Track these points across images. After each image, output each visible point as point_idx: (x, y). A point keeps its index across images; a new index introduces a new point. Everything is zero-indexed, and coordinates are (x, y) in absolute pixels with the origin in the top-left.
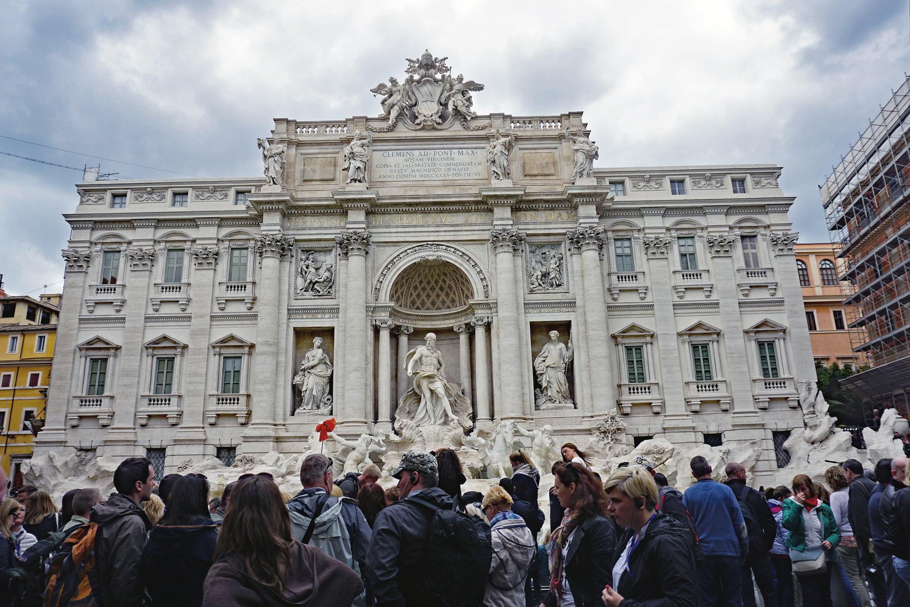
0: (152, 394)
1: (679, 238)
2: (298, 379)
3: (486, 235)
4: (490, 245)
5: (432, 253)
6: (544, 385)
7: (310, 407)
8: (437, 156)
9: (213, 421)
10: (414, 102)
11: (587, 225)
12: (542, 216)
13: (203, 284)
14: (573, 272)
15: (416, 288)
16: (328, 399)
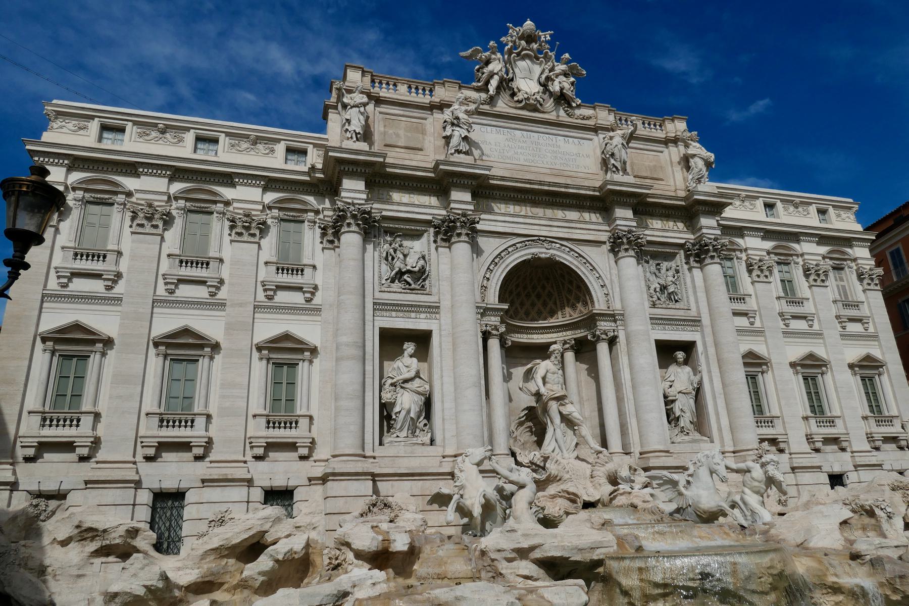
0: (162, 410)
1: (779, 263)
2: (387, 396)
3: (604, 237)
4: (607, 247)
5: (544, 250)
6: (678, 413)
7: (404, 433)
8: (541, 141)
9: (260, 451)
10: (511, 75)
11: (713, 237)
12: (657, 224)
13: (242, 263)
14: (694, 287)
15: (511, 293)
16: (425, 425)
